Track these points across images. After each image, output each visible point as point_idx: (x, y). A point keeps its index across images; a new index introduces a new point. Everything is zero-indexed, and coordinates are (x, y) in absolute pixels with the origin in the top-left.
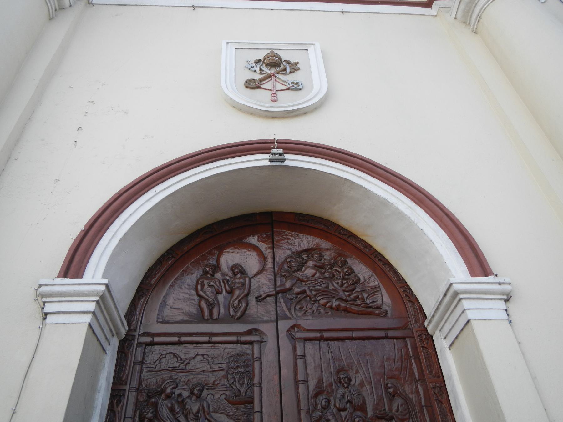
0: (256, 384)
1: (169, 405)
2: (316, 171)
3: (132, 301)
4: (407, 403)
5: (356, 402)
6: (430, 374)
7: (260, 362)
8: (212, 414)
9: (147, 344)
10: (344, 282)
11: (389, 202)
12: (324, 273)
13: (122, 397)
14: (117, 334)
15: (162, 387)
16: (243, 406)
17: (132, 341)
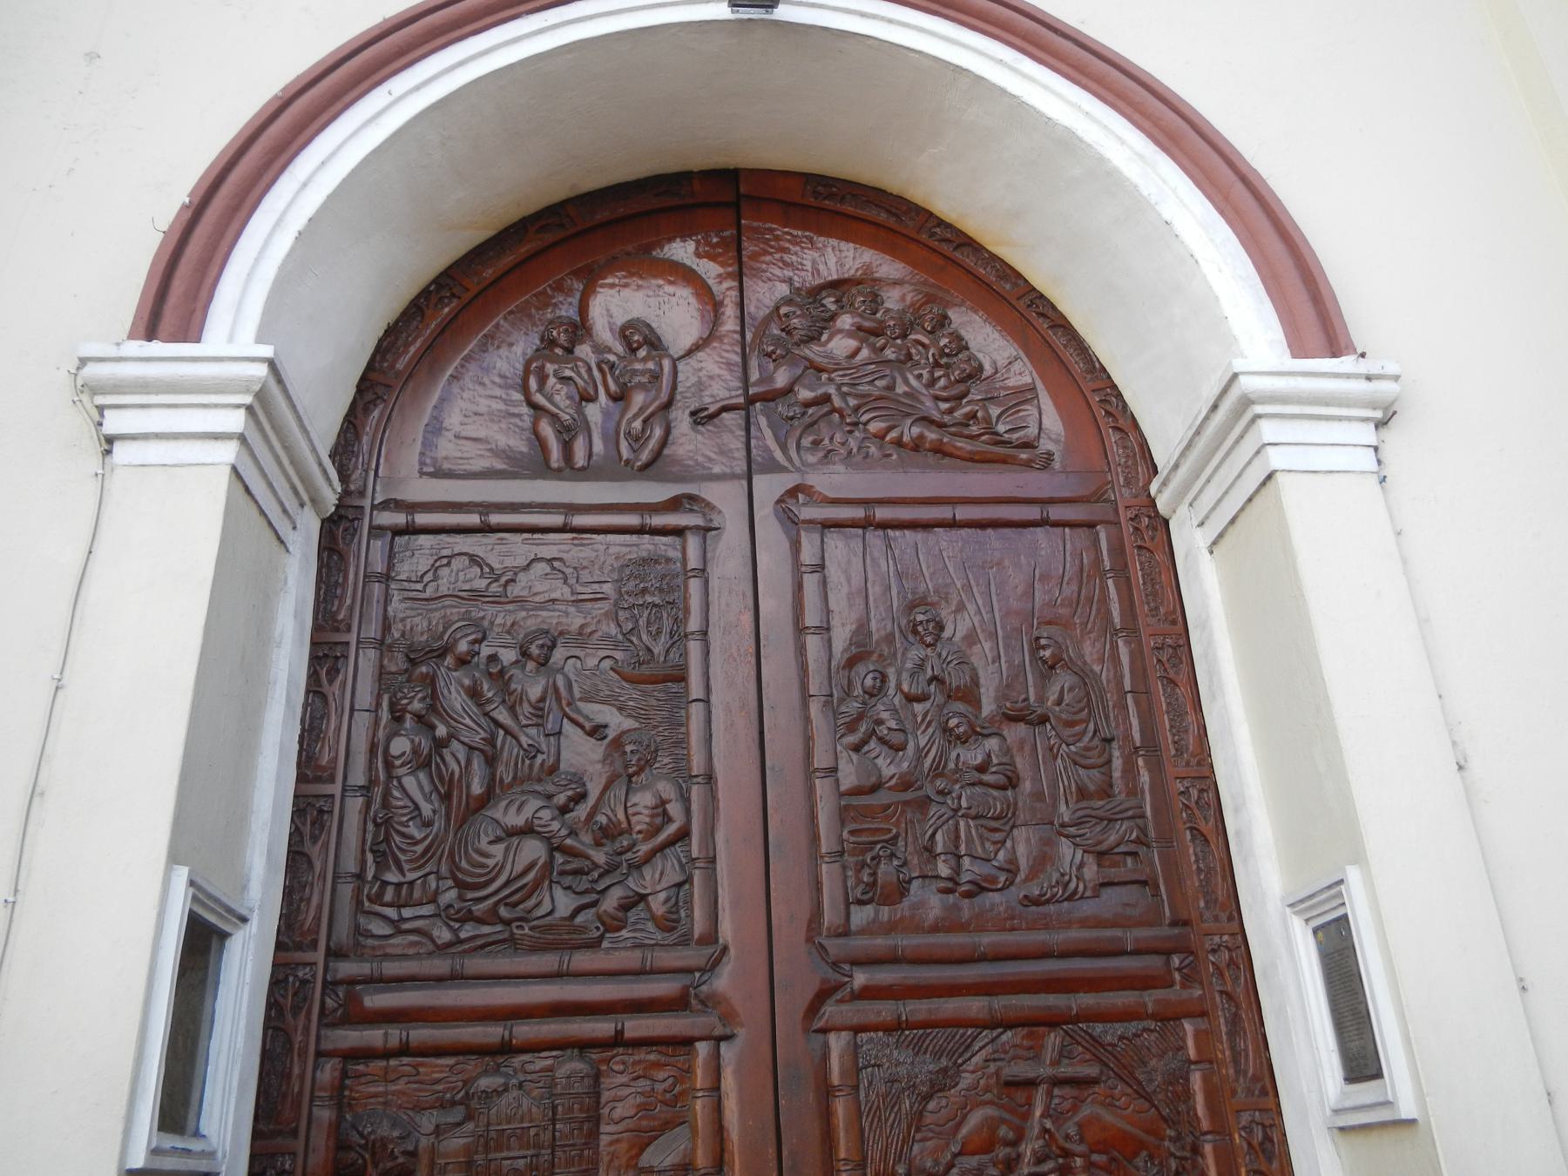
0: (693, 633)
1: (467, 682)
2: (870, 42)
3: (346, 415)
4: (1085, 684)
5: (956, 679)
6: (1153, 616)
7: (703, 579)
8: (580, 704)
9: (398, 532)
10: (937, 374)
11: (1081, 140)
12: (882, 349)
13: (342, 659)
14: (313, 501)
15: (446, 638)
16: (660, 686)
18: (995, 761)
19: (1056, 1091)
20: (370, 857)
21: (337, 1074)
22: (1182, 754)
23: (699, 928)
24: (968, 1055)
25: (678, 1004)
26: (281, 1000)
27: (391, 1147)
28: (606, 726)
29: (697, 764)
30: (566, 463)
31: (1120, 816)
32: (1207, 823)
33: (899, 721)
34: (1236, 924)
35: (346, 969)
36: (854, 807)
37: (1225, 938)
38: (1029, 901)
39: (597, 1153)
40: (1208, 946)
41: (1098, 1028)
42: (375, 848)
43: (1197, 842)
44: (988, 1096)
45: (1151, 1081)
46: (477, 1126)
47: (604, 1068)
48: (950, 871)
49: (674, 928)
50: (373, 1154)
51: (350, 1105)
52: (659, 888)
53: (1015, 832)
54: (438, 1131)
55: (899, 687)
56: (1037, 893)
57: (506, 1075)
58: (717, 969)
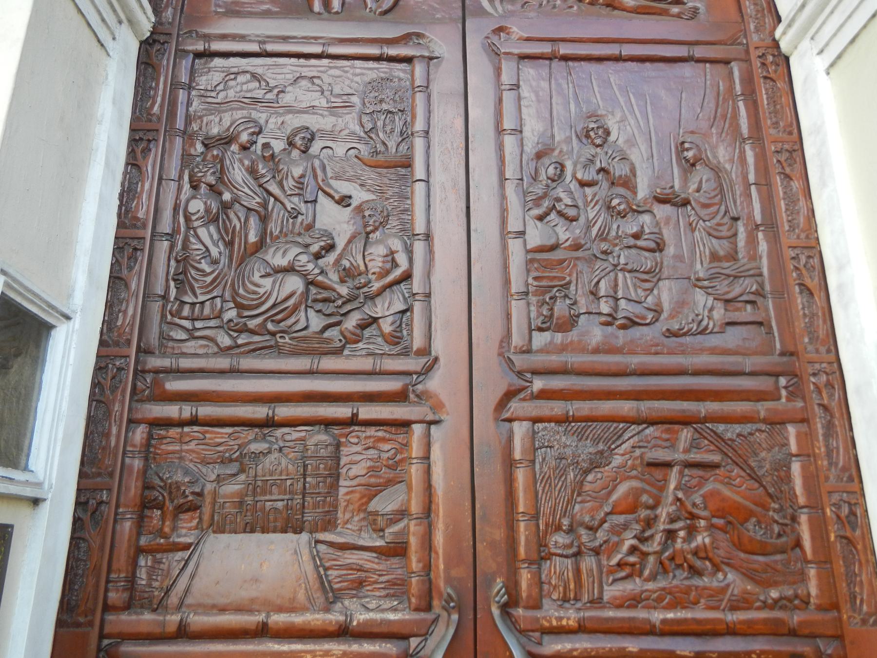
1: (246, 162)
4: (719, 177)
5: (619, 170)
6: (774, 128)
7: (426, 94)
8: (333, 182)
9: (198, 55)
13: (153, 142)
14: (130, 22)
15: (231, 130)
16: (392, 170)
17: (166, 45)
18: (647, 230)
19: (686, 471)
20: (172, 284)
21: (145, 435)
22: (794, 230)
23: (418, 342)
24: (618, 443)
25: (399, 397)
26: (102, 381)
27: (183, 488)
28: (350, 197)
29: (420, 227)
30: (325, 9)
31: (743, 274)
32: (812, 281)
33: (574, 199)
34: (833, 355)
35: (154, 362)
36: (538, 261)
37: (824, 365)
38: (671, 333)
39: (337, 500)
40: (811, 372)
41: (721, 428)
42: (176, 277)
43: (804, 294)
44: (634, 473)
45: (761, 467)
46: (248, 477)
47: (343, 440)
48: (610, 309)
49: (398, 343)
50: (170, 493)
51: (155, 458)
52: (387, 313)
53: (661, 283)
54: (219, 479)
55: (574, 176)
56: (677, 327)
57: (270, 442)
58: (430, 374)
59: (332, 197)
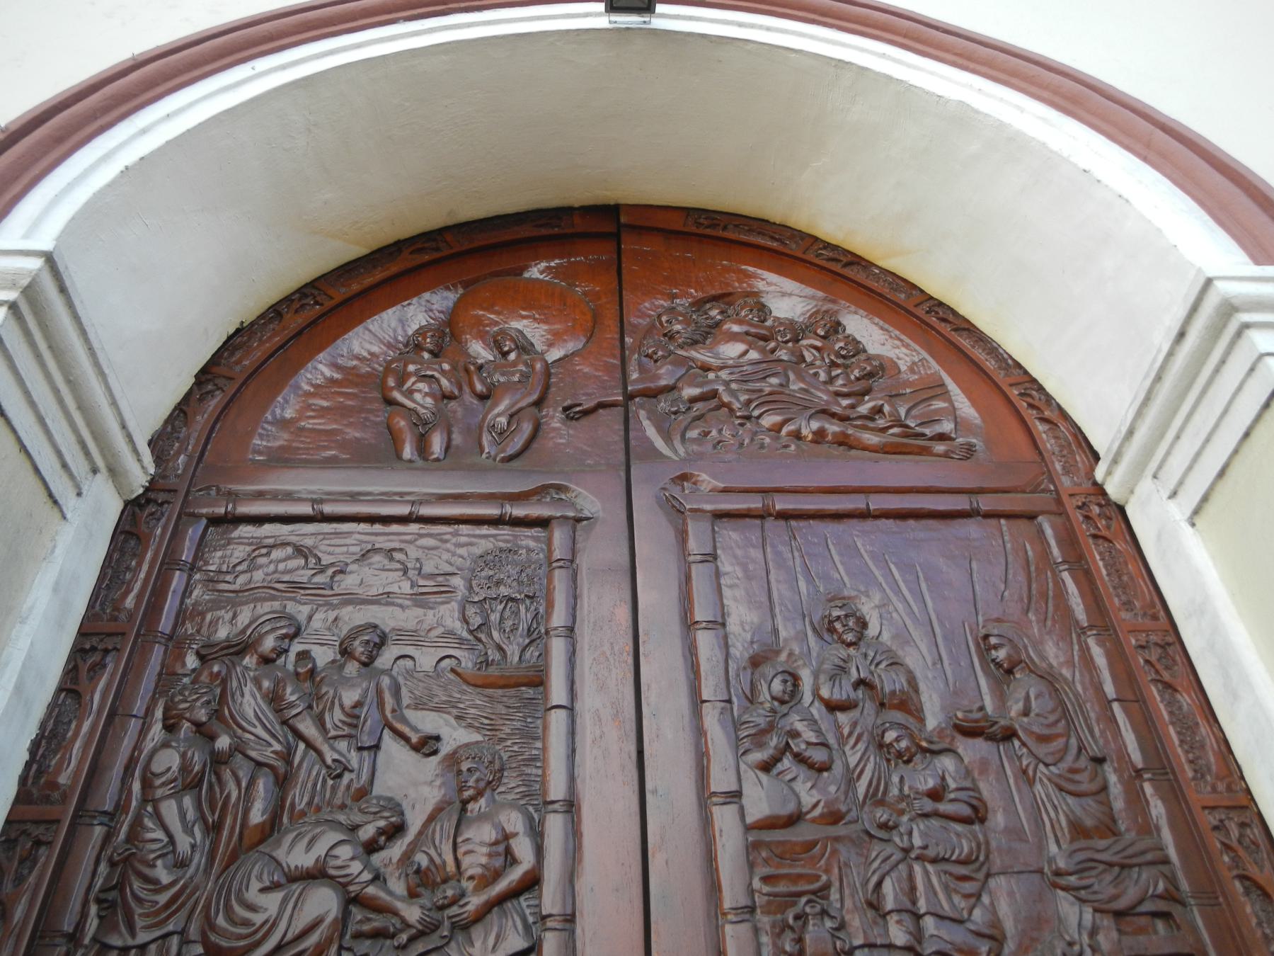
0: (556, 629)
1: (266, 684)
2: (749, 47)
3: (179, 404)
4: (1057, 690)
5: (890, 682)
8: (411, 715)
9: (215, 521)
10: (834, 373)
11: (977, 112)
12: (773, 351)
15: (248, 633)
16: (512, 691)
17: (166, 506)
18: (952, 785)
20: (93, 909)
22: (1203, 776)
28: (437, 738)
29: (557, 790)
30: (420, 456)
31: (1135, 861)
32: (1261, 871)
33: (819, 732)
36: (768, 845)
42: (103, 896)
43: (1254, 896)
48: (908, 937)
53: (992, 883)
55: (816, 694)
59: (406, 739)
